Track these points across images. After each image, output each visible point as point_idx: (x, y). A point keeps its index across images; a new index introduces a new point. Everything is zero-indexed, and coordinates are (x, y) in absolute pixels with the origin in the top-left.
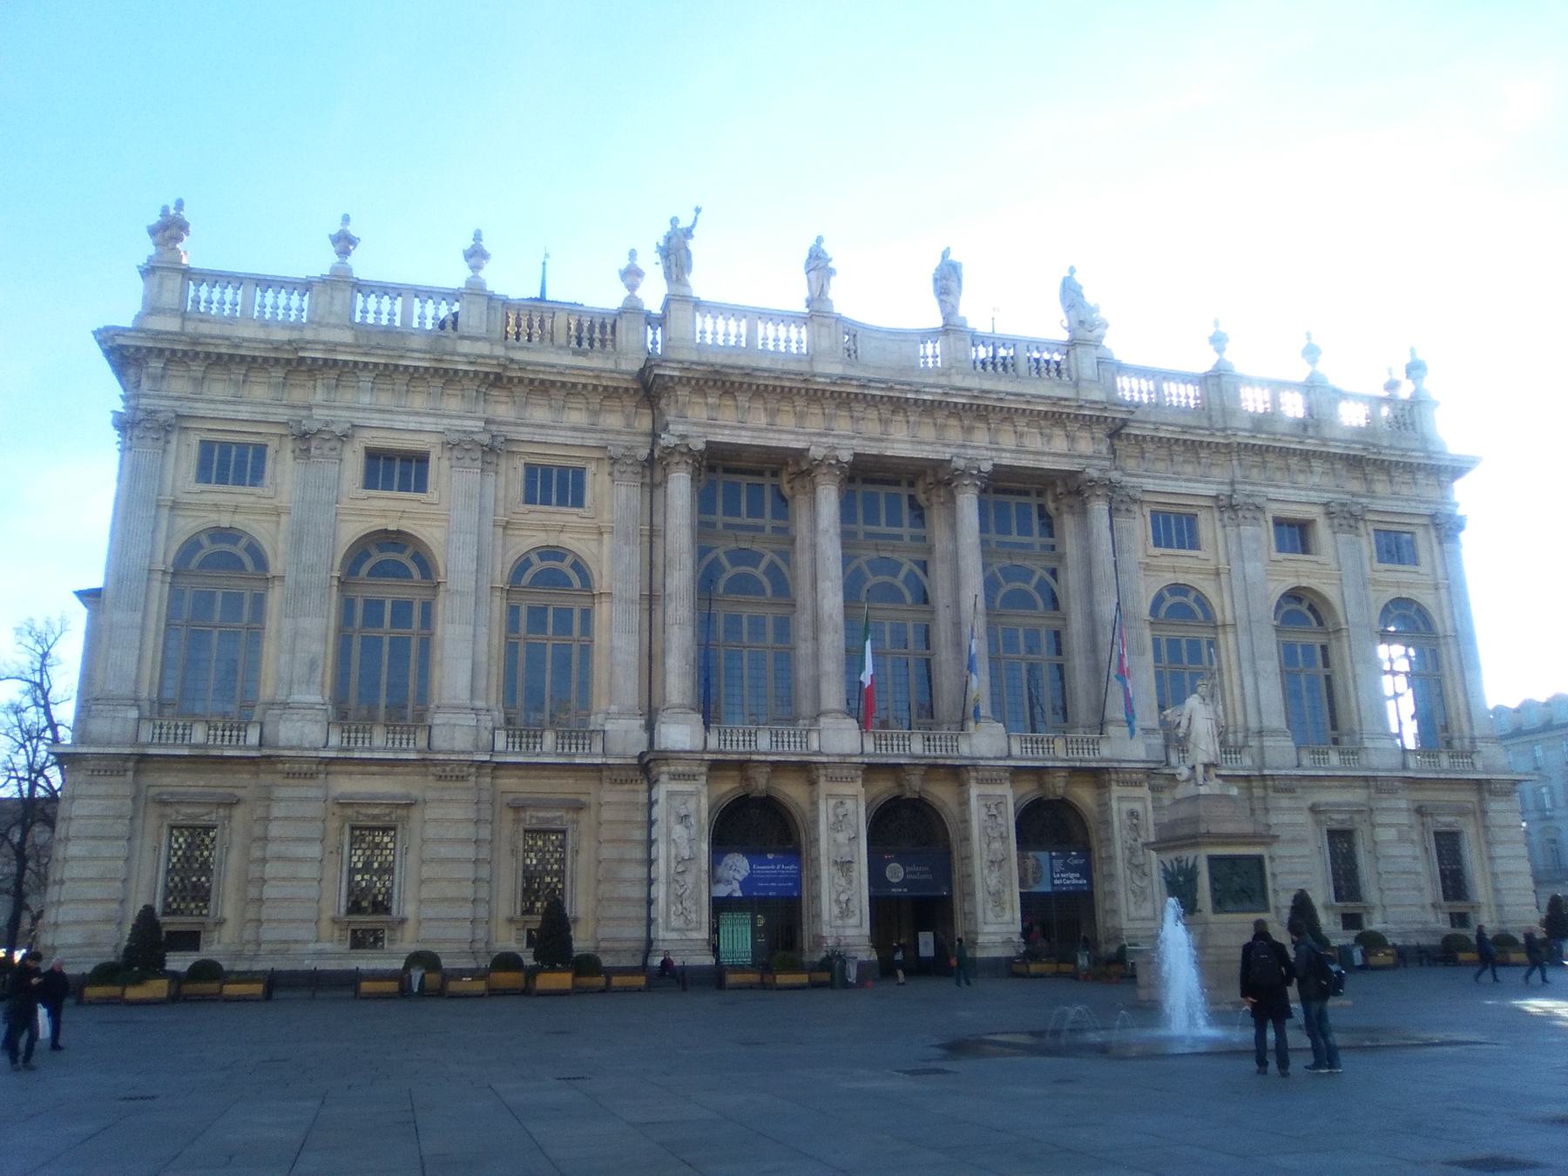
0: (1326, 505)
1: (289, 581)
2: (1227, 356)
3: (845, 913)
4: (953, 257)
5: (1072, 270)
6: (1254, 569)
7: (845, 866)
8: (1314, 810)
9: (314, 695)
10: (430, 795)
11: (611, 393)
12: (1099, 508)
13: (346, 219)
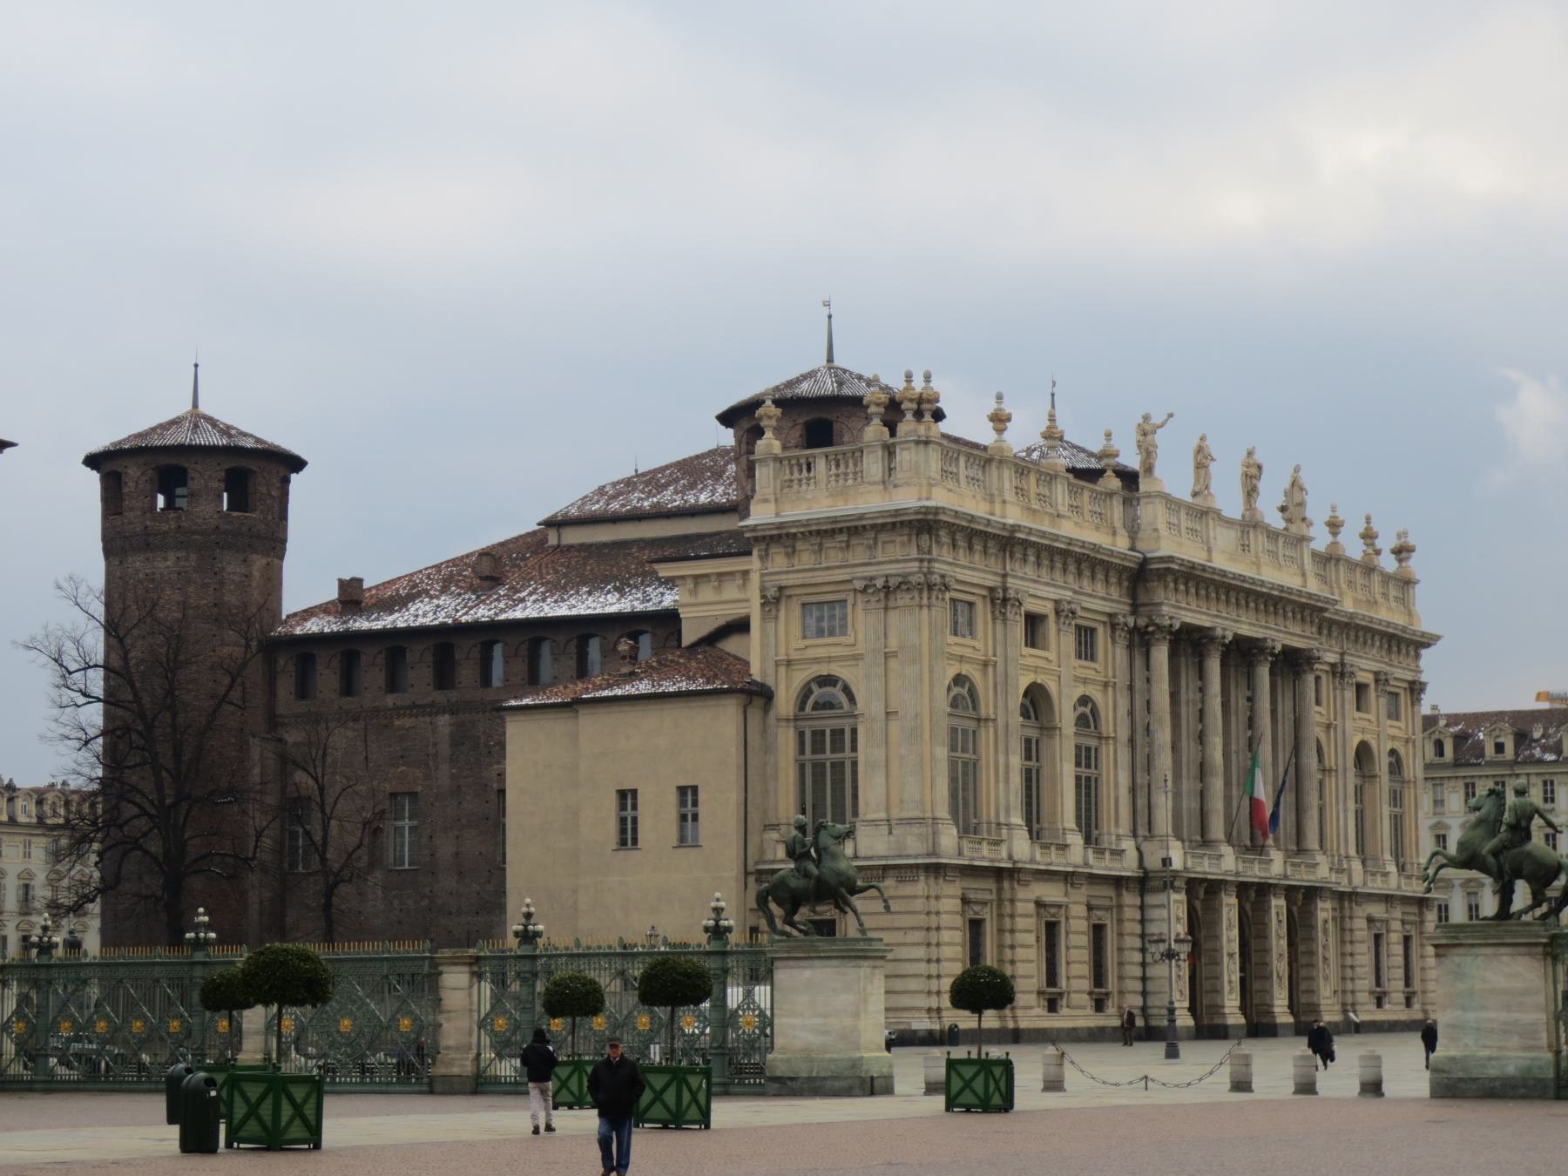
0: (1377, 674)
1: (1000, 722)
2: (1340, 538)
3: (1230, 992)
4: (1259, 457)
5: (1297, 469)
6: (1349, 724)
7: (1231, 955)
8: (1370, 920)
9: (1017, 819)
10: (1072, 898)
11: (1121, 570)
12: (1310, 678)
13: (999, 397)
